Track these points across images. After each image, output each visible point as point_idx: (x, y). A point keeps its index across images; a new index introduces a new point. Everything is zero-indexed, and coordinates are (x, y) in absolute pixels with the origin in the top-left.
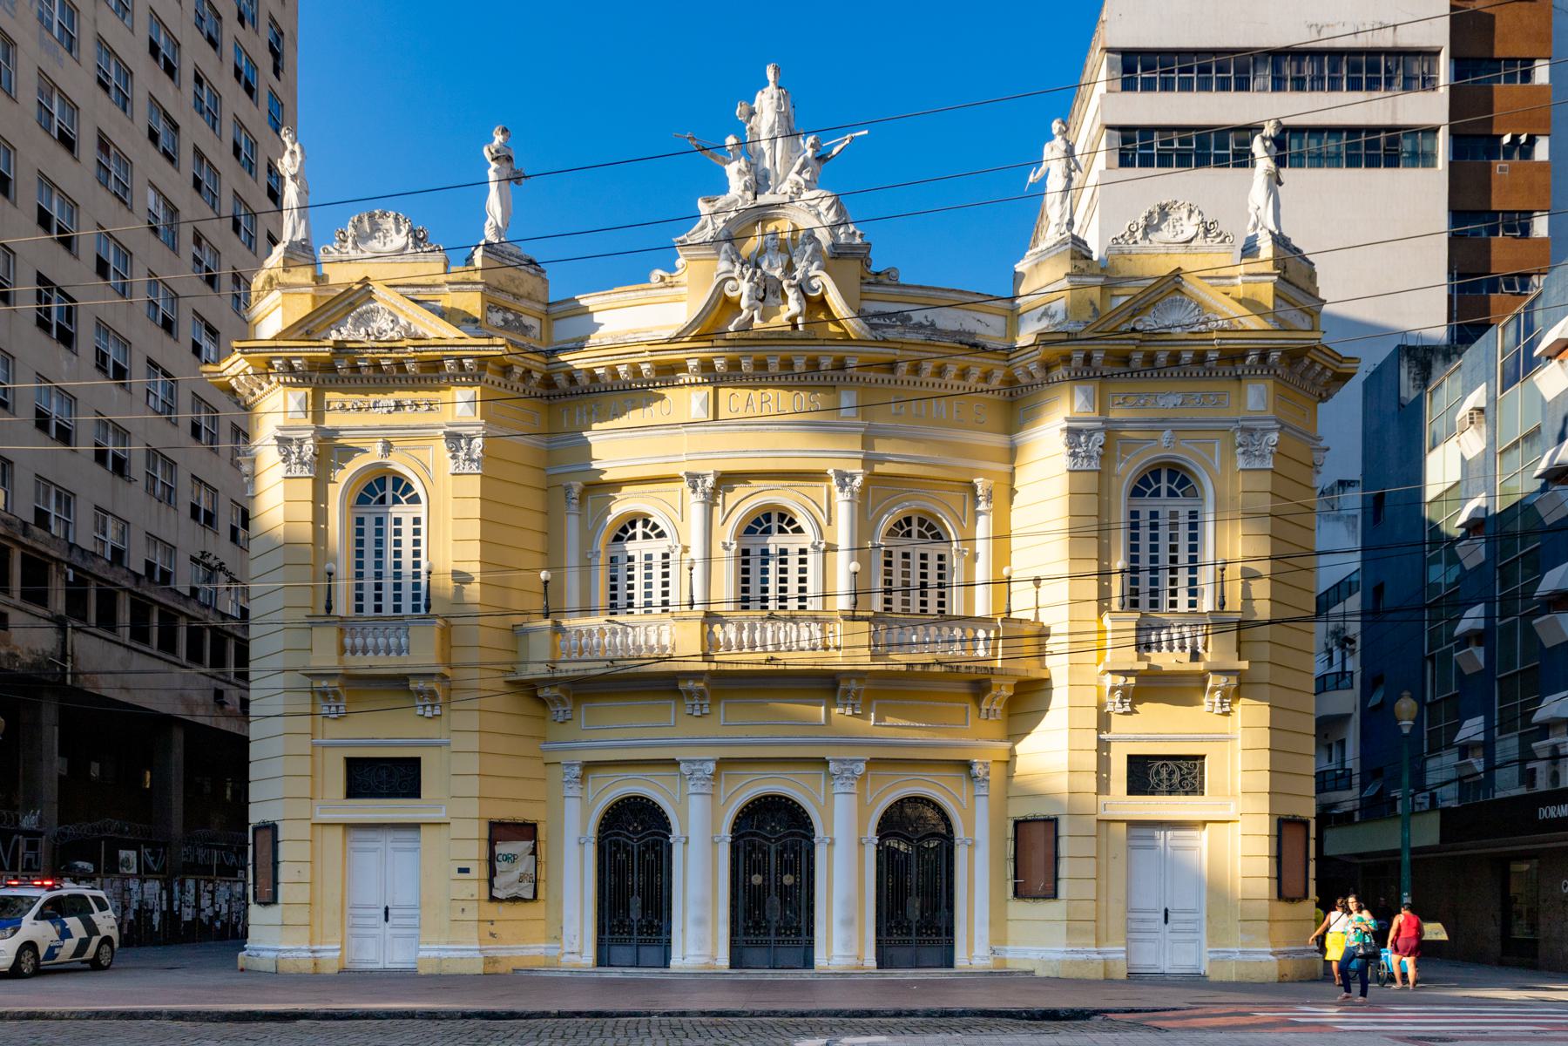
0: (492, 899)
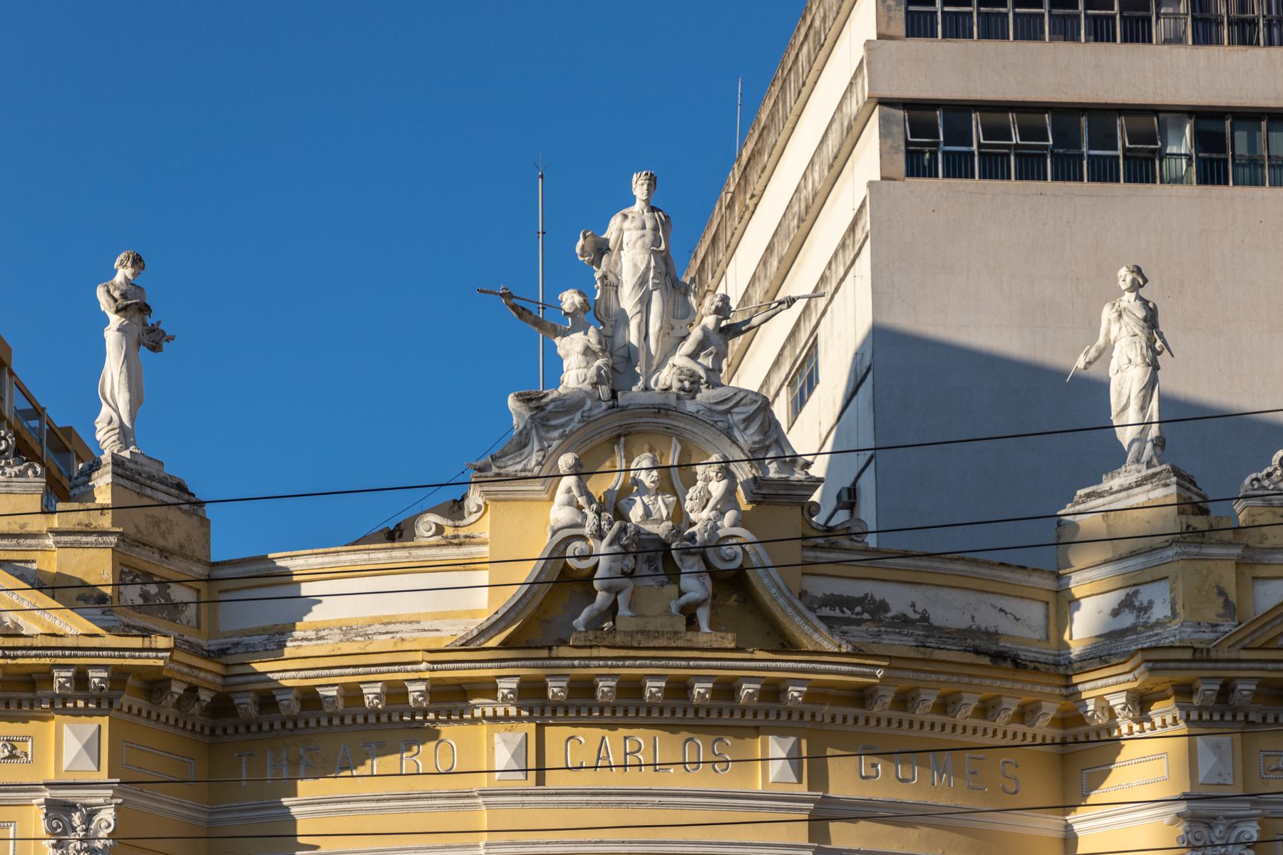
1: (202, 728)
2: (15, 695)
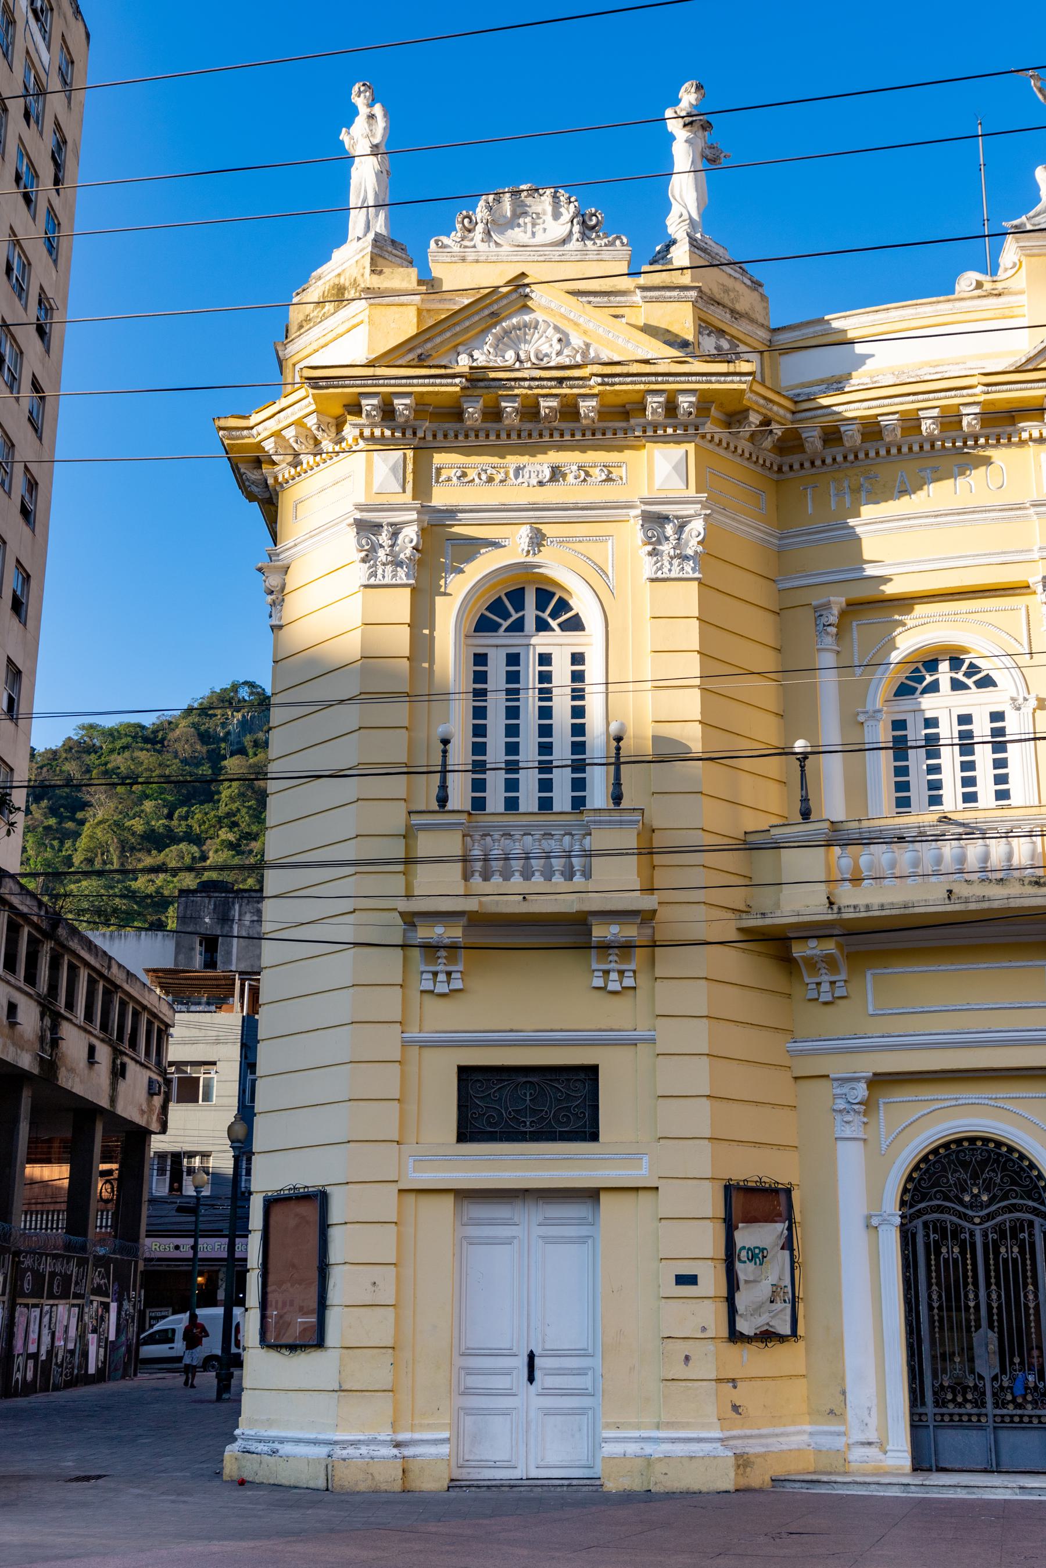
0: (735, 1336)
1: (772, 465)
2: (610, 424)
